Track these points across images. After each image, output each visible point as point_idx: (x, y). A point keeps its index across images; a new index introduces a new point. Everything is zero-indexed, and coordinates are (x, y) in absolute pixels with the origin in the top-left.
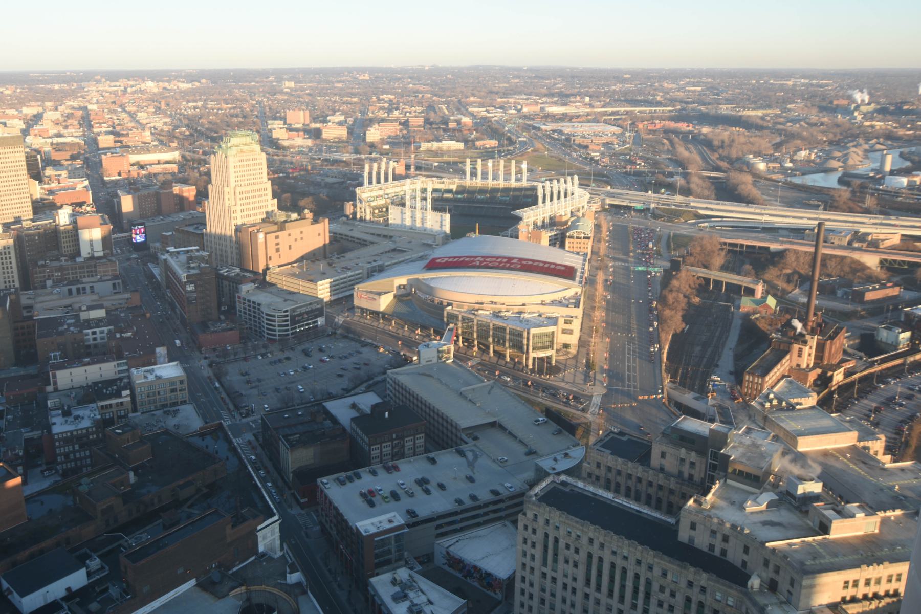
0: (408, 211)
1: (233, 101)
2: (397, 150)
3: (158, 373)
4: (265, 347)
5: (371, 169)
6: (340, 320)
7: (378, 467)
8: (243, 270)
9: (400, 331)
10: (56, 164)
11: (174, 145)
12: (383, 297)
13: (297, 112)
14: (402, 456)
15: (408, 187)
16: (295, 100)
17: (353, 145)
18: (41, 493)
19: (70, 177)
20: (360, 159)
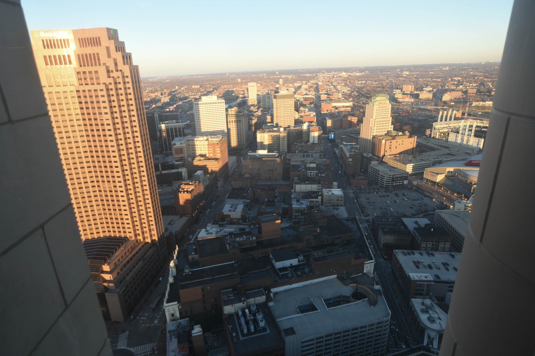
0: (460, 136)
1: (379, 81)
2: (459, 105)
3: (333, 192)
4: (378, 189)
5: (443, 114)
6: (415, 183)
7: (424, 253)
8: (374, 155)
9: (445, 193)
10: (304, 106)
11: (351, 99)
12: (439, 176)
13: (408, 86)
14: (437, 250)
15: (462, 124)
16: (408, 80)
17: (434, 102)
18: (286, 228)
19: (309, 111)
20: (438, 109)
